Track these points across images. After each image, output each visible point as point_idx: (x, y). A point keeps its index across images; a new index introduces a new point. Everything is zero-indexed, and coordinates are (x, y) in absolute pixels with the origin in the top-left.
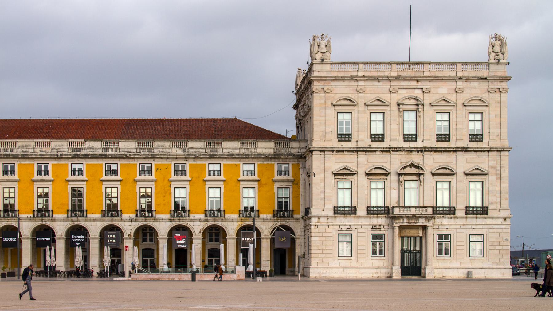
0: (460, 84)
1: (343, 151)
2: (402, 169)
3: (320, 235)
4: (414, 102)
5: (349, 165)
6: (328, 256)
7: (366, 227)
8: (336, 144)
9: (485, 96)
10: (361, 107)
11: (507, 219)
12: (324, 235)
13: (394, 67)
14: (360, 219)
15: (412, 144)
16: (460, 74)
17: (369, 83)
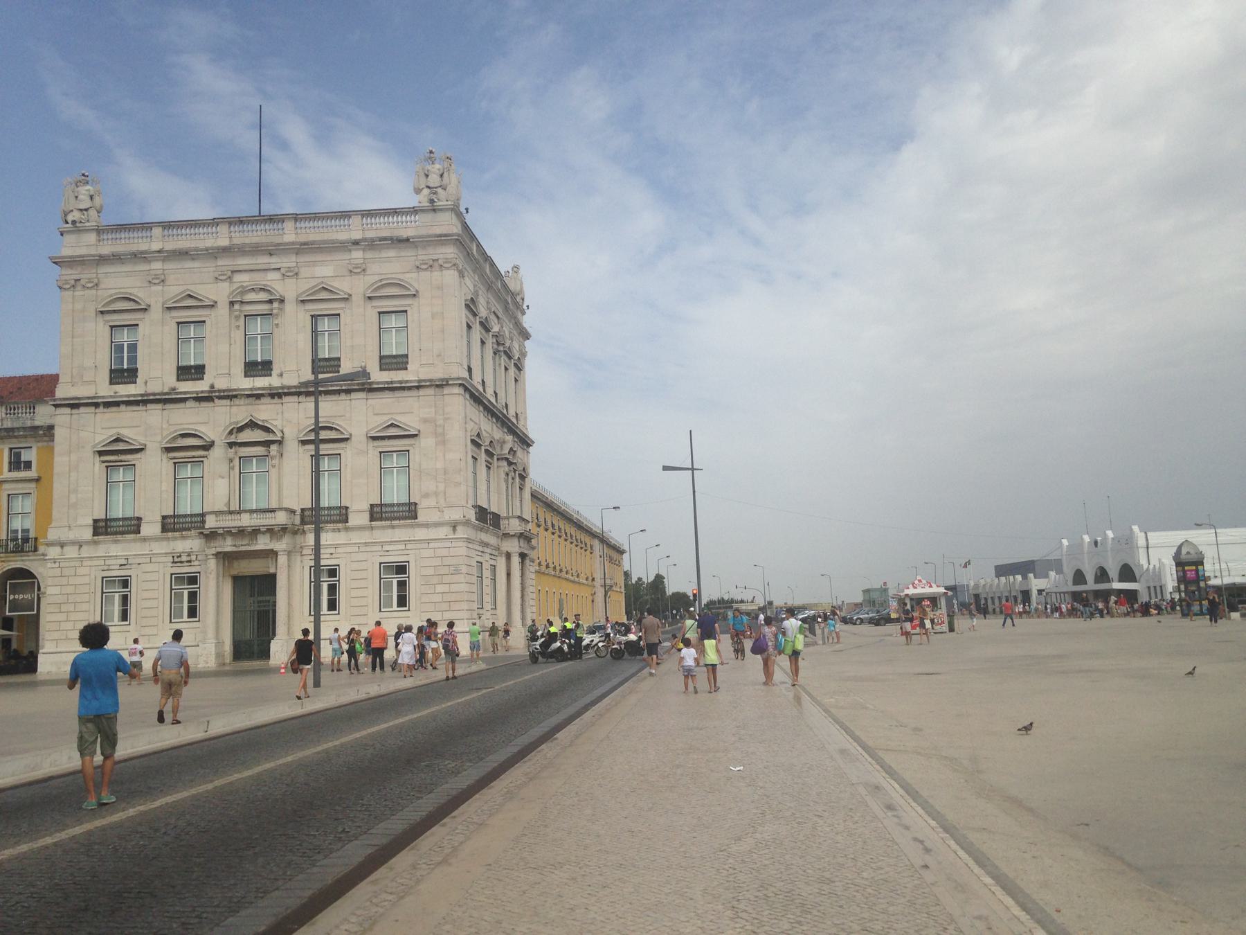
0: (357, 255)
1: (117, 404)
2: (231, 433)
3: (64, 581)
4: (263, 296)
5: (127, 433)
7: (159, 559)
8: (105, 390)
9: (411, 278)
10: (156, 313)
11: (459, 528)
12: (72, 580)
13: (223, 229)
15: (261, 382)
16: (357, 235)
17: (170, 266)
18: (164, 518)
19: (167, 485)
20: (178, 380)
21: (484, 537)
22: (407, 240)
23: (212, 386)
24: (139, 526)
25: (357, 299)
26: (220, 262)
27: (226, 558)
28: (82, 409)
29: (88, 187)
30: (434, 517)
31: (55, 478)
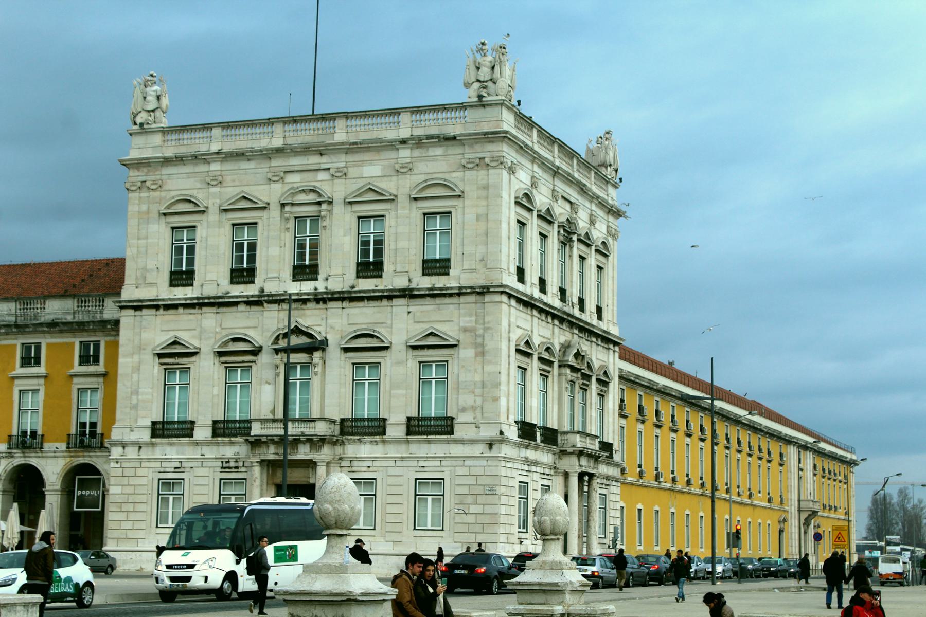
0: (405, 153)
1: (175, 307)
2: (277, 338)
3: (125, 481)
4: (312, 197)
5: (184, 337)
6: (137, 525)
7: (210, 464)
8: (166, 293)
9: (456, 177)
10: (213, 215)
12: (133, 481)
13: (278, 128)
14: (199, 448)
15: (307, 287)
16: (405, 133)
17: (229, 166)
18: (215, 422)
19: (218, 390)
20: (232, 282)
21: (531, 454)
22: (454, 138)
23: (262, 290)
24: (193, 430)
25: (403, 200)
26: (274, 163)
27: (269, 465)
28: (145, 311)
29: (156, 88)
30: (471, 433)
31: (120, 379)
